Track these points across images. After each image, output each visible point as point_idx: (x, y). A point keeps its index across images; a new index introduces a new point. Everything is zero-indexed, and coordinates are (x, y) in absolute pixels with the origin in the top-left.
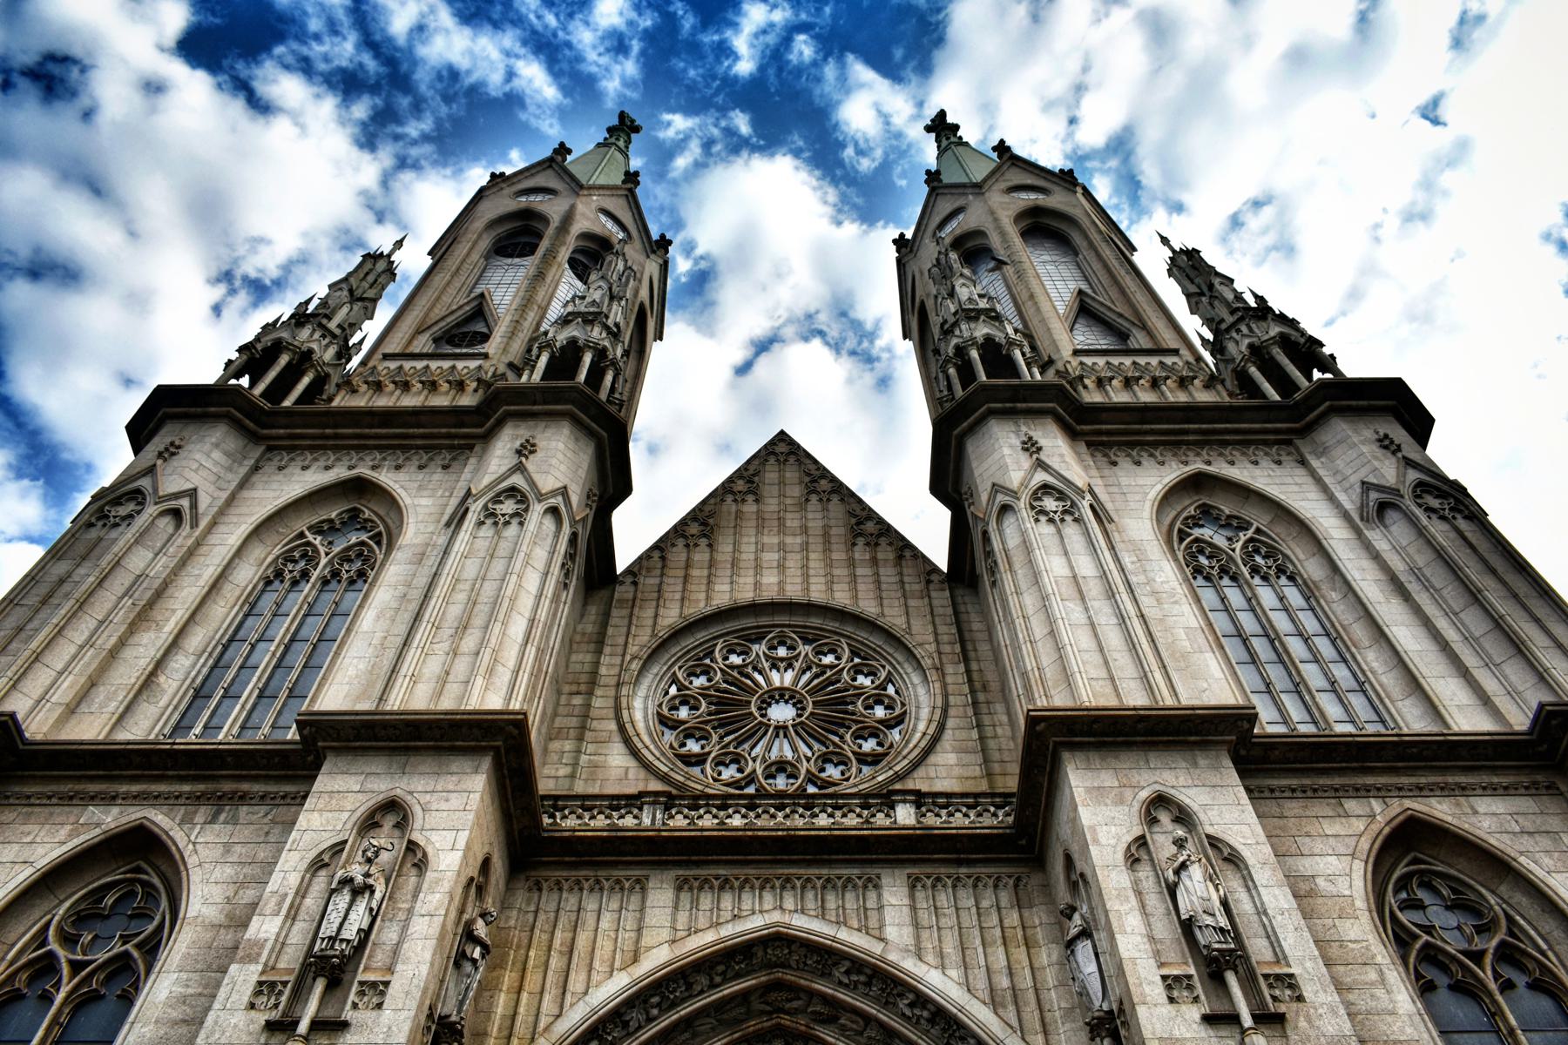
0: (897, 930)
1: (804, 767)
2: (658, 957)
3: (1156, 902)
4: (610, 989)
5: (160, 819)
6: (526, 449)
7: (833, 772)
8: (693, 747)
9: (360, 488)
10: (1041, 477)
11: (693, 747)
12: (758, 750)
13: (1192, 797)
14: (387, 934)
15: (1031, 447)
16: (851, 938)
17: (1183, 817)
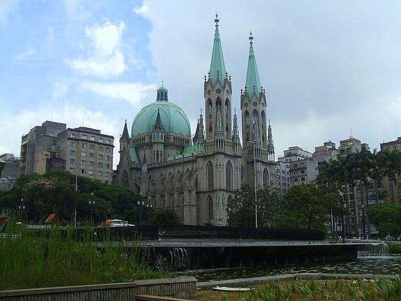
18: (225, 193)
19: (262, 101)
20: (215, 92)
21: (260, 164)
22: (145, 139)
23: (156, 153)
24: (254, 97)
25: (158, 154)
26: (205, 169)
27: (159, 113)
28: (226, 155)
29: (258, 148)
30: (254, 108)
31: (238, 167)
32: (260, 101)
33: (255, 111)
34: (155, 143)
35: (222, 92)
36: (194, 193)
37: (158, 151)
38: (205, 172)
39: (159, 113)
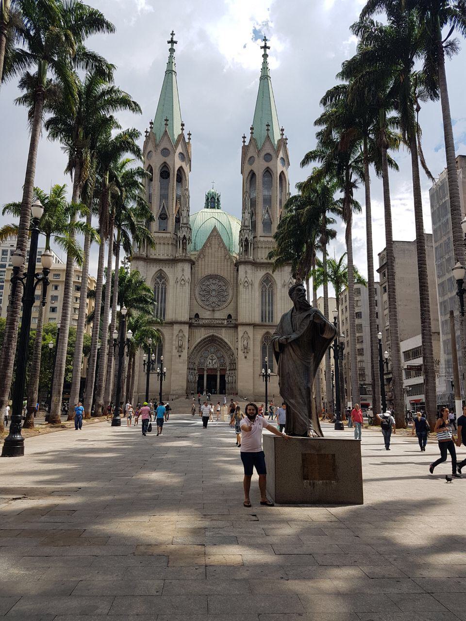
0: (223, 335)
1: (216, 302)
2: (203, 337)
3: (242, 342)
4: (199, 340)
5: (160, 328)
6: (183, 270)
7: (219, 303)
8: (203, 298)
10: (246, 279)
11: (203, 298)
12: (211, 300)
13: (248, 332)
14: (184, 343)
15: (246, 272)
16: (219, 336)
17: (247, 333)
19: (281, 155)
21: (249, 268)
32: (277, 152)
35: (172, 152)
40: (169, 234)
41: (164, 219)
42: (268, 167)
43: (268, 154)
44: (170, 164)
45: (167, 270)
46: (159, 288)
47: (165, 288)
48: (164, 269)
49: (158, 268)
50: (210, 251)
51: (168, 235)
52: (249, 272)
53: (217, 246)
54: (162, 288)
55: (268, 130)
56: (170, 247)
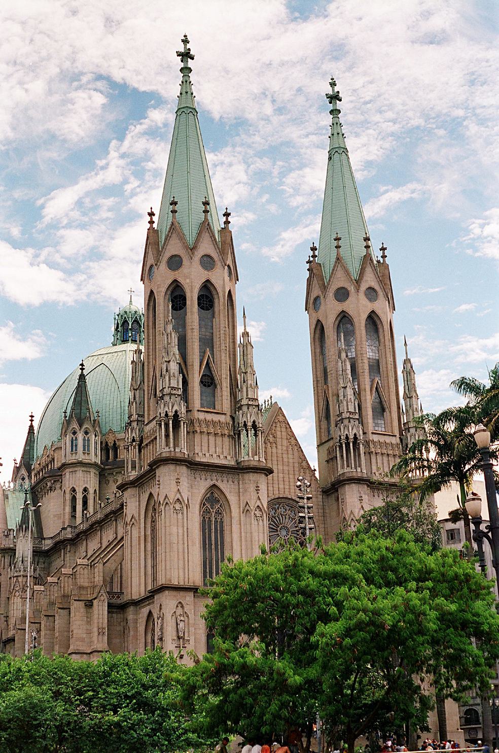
9: (214, 485)
18: (189, 598)
20: (163, 266)
22: (53, 459)
23: (68, 497)
24: (340, 273)
25: (74, 499)
26: (142, 525)
27: (82, 377)
28: (193, 465)
29: (347, 438)
30: (338, 307)
31: (253, 504)
33: (344, 319)
34: (64, 466)
36: (101, 610)
37: (74, 490)
38: (143, 533)
39: (82, 377)
40: (223, 416)
41: (209, 386)
42: (373, 312)
43: (371, 289)
44: (216, 285)
45: (227, 486)
46: (210, 521)
47: (222, 522)
48: (219, 484)
49: (209, 483)
50: (274, 450)
51: (222, 418)
52: (365, 497)
53: (285, 442)
54: (216, 522)
55: (367, 247)
56: (226, 439)
